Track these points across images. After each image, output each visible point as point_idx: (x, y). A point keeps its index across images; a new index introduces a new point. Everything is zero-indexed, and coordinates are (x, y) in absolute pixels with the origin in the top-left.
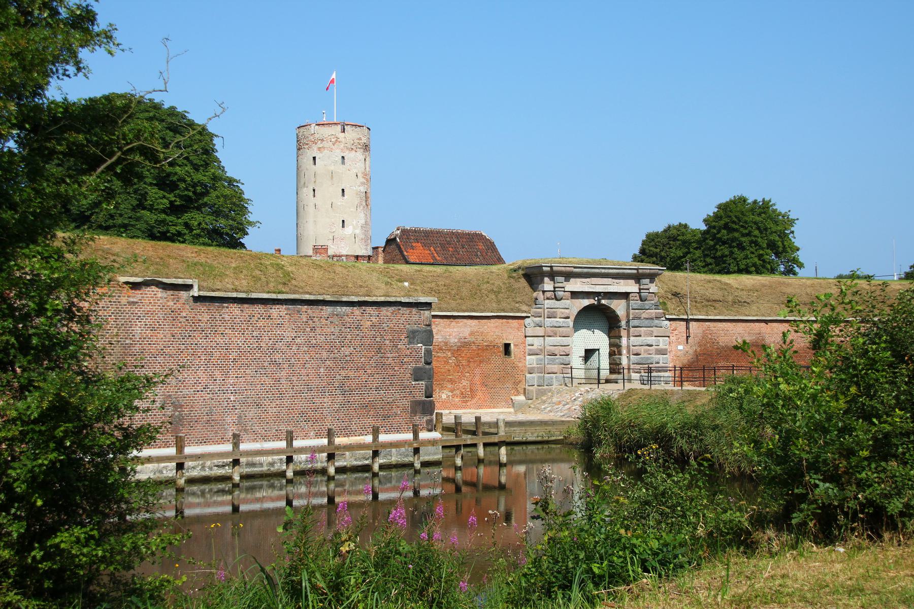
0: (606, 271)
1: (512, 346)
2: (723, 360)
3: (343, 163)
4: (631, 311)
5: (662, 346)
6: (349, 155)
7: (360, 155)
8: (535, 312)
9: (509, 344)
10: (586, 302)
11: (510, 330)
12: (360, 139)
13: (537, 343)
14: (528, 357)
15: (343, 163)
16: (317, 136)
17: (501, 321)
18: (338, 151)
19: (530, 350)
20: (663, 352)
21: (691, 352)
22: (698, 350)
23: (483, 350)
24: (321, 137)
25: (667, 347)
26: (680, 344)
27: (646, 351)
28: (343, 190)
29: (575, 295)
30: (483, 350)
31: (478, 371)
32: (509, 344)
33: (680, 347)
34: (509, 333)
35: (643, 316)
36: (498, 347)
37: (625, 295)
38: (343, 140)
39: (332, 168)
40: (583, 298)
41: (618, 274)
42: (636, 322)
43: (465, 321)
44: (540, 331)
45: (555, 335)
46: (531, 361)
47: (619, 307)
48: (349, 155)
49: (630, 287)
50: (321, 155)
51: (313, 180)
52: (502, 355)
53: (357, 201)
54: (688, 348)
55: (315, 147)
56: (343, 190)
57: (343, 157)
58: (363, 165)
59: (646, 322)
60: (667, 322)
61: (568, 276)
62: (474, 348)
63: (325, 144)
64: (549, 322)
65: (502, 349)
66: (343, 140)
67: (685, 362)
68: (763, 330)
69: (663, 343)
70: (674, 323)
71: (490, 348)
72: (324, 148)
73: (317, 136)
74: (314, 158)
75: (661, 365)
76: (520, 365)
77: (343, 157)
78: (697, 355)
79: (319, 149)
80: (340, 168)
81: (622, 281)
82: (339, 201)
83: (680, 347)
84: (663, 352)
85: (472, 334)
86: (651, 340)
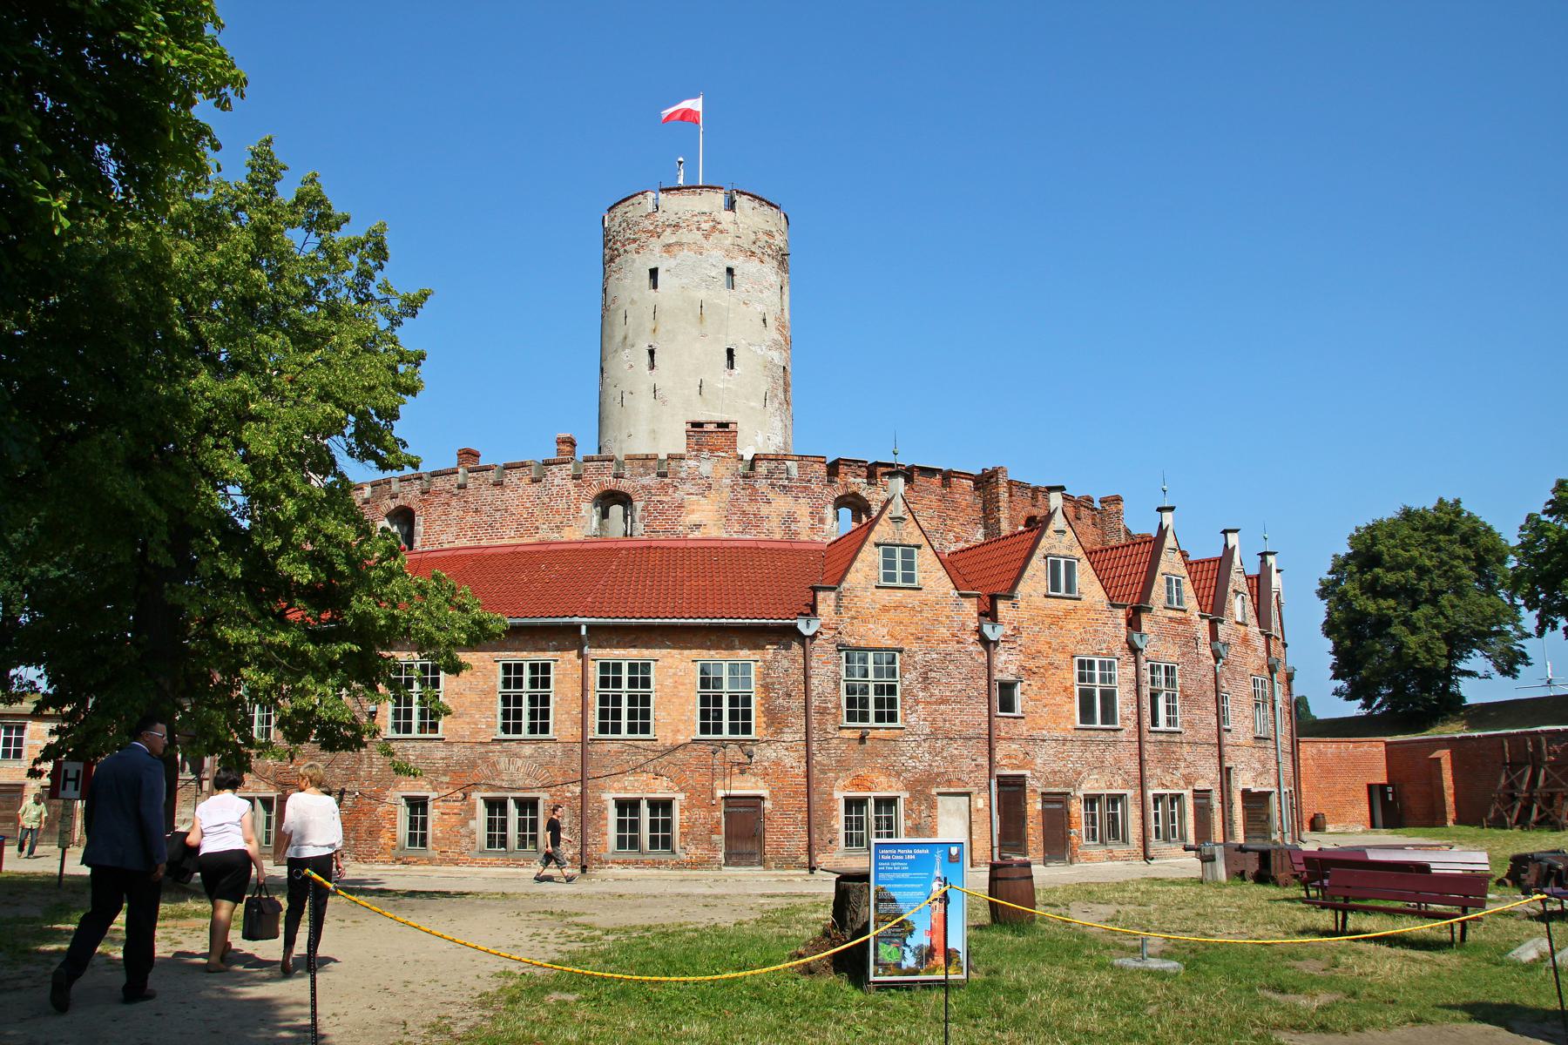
7: (769, 272)
12: (770, 234)
18: (718, 253)
24: (673, 219)
28: (730, 352)
38: (731, 228)
39: (702, 294)
50: (672, 263)
51: (650, 325)
53: (764, 385)
55: (656, 244)
56: (730, 352)
57: (730, 271)
58: (776, 299)
63: (684, 235)
66: (731, 228)
72: (680, 244)
74: (654, 273)
77: (730, 271)
79: (668, 248)
80: (721, 297)
82: (719, 377)
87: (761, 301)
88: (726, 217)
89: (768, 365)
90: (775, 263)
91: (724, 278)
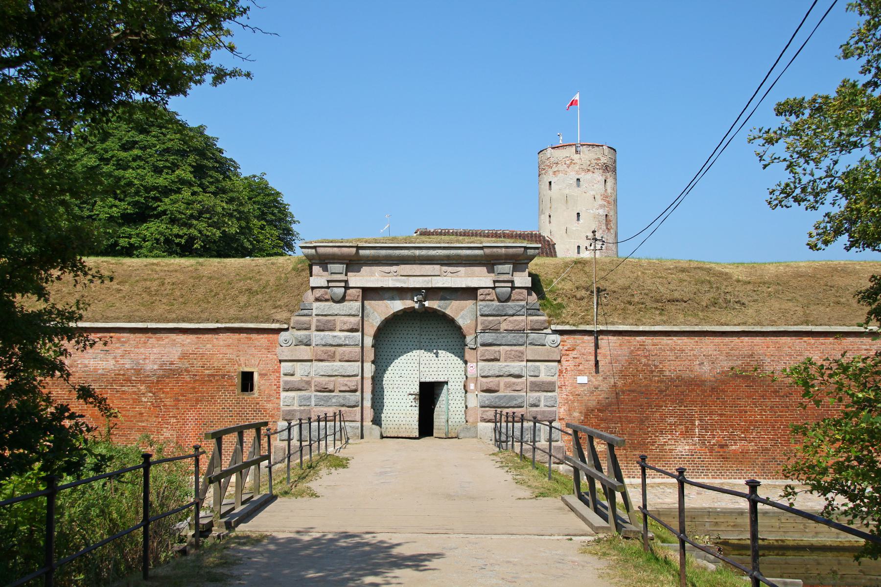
0: (424, 252)
1: (256, 377)
2: (673, 401)
3: (578, 186)
4: (480, 319)
5: (544, 377)
6: (585, 177)
7: (599, 176)
8: (297, 322)
9: (252, 373)
10: (398, 305)
11: (253, 351)
12: (599, 159)
13: (300, 370)
14: (283, 394)
15: (578, 186)
16: (552, 160)
17: (237, 336)
19: (286, 382)
20: (548, 387)
21: (604, 386)
22: (620, 383)
23: (203, 382)
25: (555, 378)
26: (581, 373)
27: (508, 386)
29: (369, 293)
30: (203, 382)
31: (191, 415)
32: (252, 373)
33: (582, 379)
34: (251, 355)
35: (504, 326)
36: (230, 378)
37: (470, 293)
38: (579, 162)
39: (567, 191)
40: (393, 299)
41: (448, 257)
42: (488, 337)
43: (173, 336)
44: (304, 352)
45: (332, 358)
46: (288, 400)
47: (462, 313)
48: (585, 177)
49: (478, 278)
51: (549, 206)
52: (238, 390)
54: (598, 380)
55: (550, 172)
57: (578, 180)
58: (602, 186)
59: (510, 337)
60: (557, 338)
61: (354, 262)
62: (188, 378)
63: (561, 167)
64: (317, 337)
65: (237, 381)
67: (593, 404)
68: (758, 350)
69: (545, 372)
70: (570, 340)
71: (217, 378)
72: (558, 171)
73: (552, 160)
74: (550, 183)
75: (542, 408)
76: (269, 406)
78: (617, 393)
81: (462, 269)
82: (574, 226)
83: (582, 379)
84: (548, 387)
85: (184, 356)
86: (516, 367)
87: (593, 190)
88: (576, 157)
89: (596, 217)
90: (601, 171)
91: (575, 184)
